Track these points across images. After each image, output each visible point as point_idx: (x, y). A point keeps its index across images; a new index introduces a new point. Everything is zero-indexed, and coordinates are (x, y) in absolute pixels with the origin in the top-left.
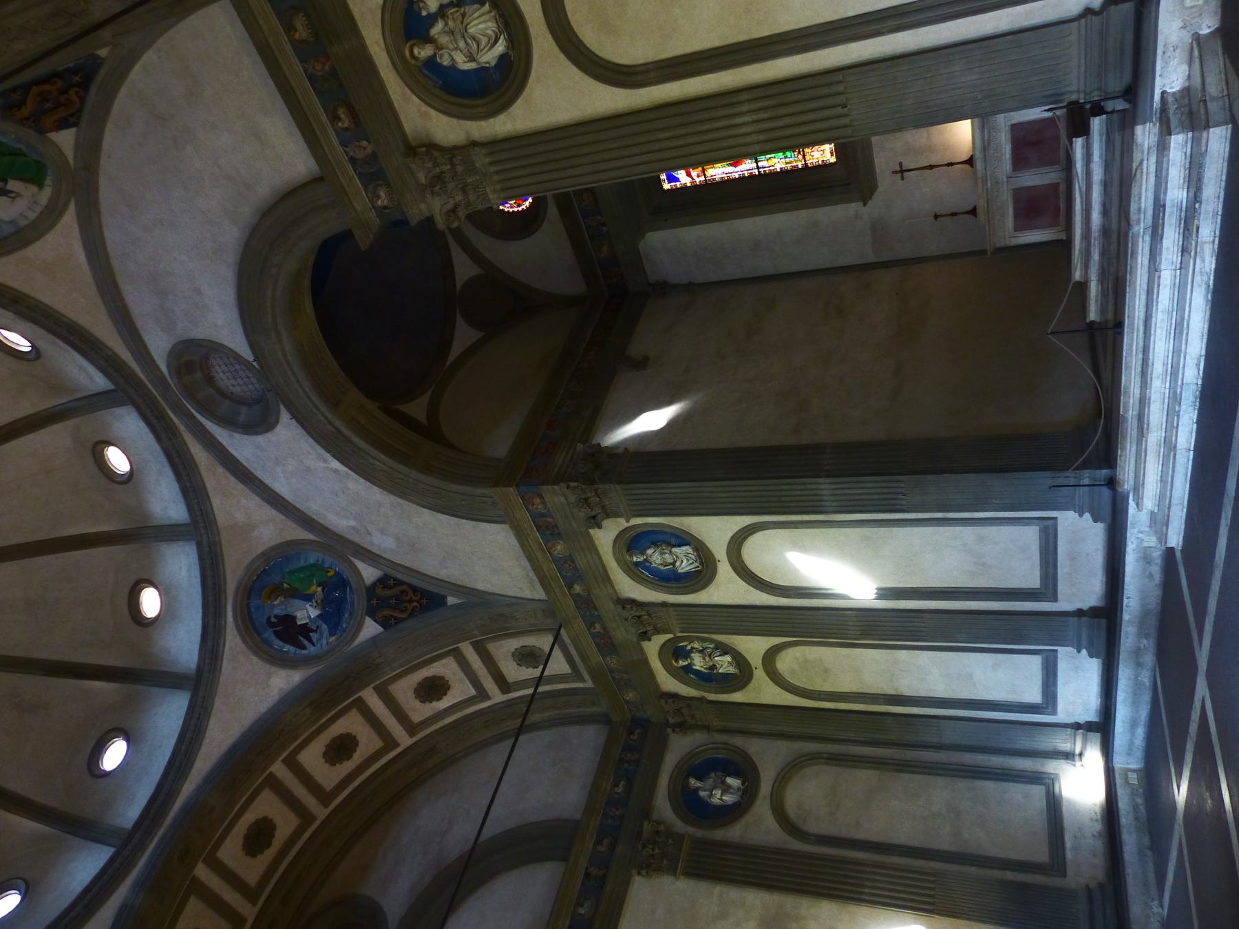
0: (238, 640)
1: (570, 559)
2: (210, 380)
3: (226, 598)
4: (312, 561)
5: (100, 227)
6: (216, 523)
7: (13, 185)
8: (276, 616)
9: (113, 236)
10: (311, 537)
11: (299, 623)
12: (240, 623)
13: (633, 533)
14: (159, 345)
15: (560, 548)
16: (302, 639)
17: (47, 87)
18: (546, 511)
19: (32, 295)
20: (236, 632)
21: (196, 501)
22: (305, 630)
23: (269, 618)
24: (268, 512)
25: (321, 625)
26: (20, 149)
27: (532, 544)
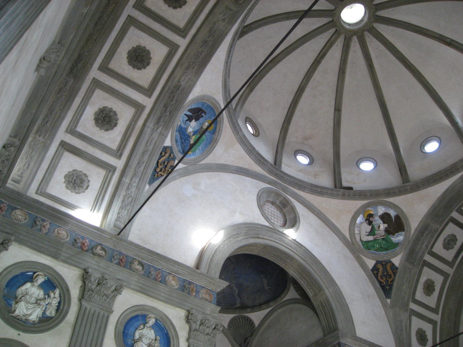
0: (217, 98)
1: (164, 281)
2: (273, 203)
3: (226, 114)
4: (197, 151)
5: (340, 239)
6: (240, 143)
7: (371, 238)
8: (203, 116)
9: (336, 238)
10: (203, 162)
11: (194, 120)
12: (218, 107)
13: (171, 334)
14: (300, 209)
15: (174, 283)
16: (191, 114)
17: (391, 280)
18: (201, 297)
19: (340, 200)
20: (219, 101)
21: (249, 148)
22: (190, 119)
23: (205, 113)
24: (222, 161)
25: (184, 125)
26: (378, 252)
27: (184, 271)
